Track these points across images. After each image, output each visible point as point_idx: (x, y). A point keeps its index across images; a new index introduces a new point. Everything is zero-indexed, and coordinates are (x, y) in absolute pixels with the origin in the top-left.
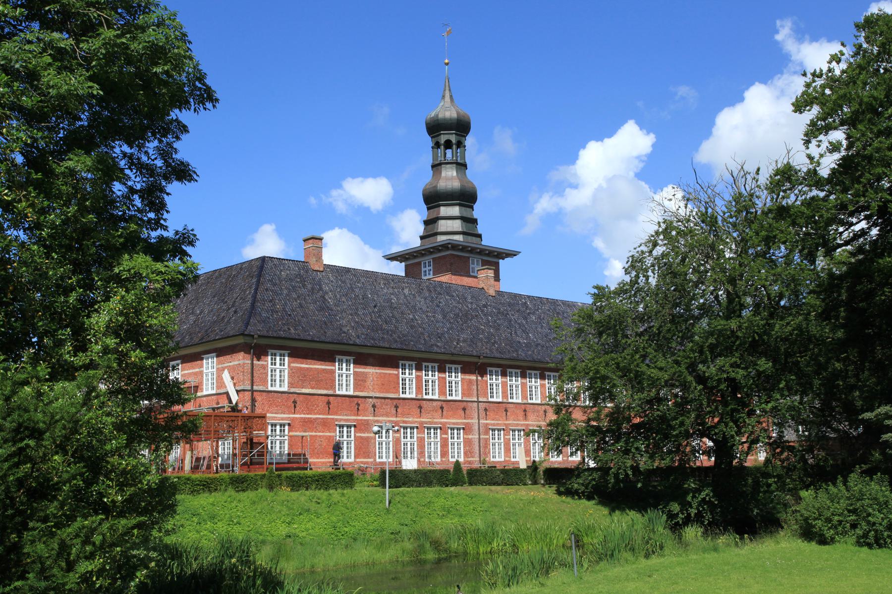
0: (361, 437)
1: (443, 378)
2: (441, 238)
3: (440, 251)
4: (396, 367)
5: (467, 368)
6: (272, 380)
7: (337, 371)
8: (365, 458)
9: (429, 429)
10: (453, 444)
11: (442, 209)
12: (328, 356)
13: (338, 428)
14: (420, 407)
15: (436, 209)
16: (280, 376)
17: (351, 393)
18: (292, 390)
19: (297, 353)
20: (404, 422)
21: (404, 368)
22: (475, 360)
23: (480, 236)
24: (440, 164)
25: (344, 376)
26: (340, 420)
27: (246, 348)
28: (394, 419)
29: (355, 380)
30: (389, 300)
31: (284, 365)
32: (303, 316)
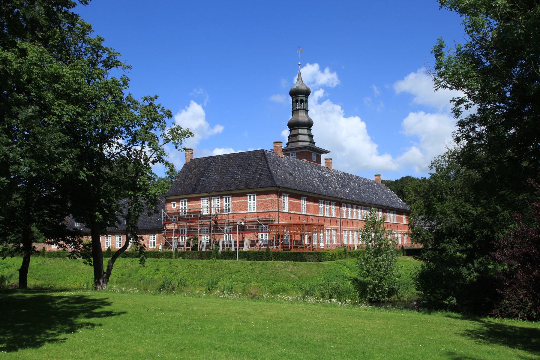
4: (318, 202)
11: (300, 130)
23: (314, 143)
24: (298, 110)
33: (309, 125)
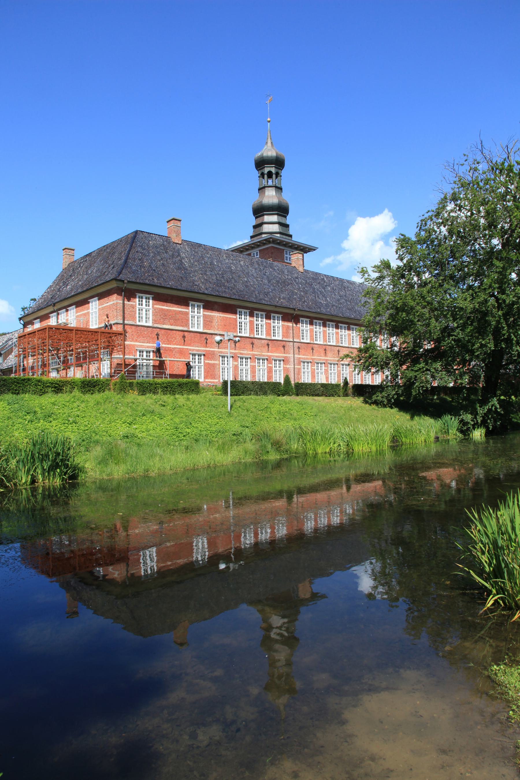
0: (209, 363)
1: (269, 323)
3: (264, 244)
4: (235, 313)
5: (286, 317)
6: (139, 317)
7: (190, 313)
8: (212, 379)
9: (259, 359)
10: (276, 371)
12: (184, 302)
13: (191, 356)
14: (253, 344)
15: (261, 218)
16: (146, 314)
17: (201, 330)
18: (156, 325)
19: (159, 298)
20: (241, 354)
21: (240, 314)
22: (292, 312)
23: (291, 236)
24: (264, 187)
25: (196, 317)
26: (193, 350)
27: (119, 291)
28: (233, 351)
29: (204, 320)
30: (230, 267)
31: (149, 306)
32: (164, 272)
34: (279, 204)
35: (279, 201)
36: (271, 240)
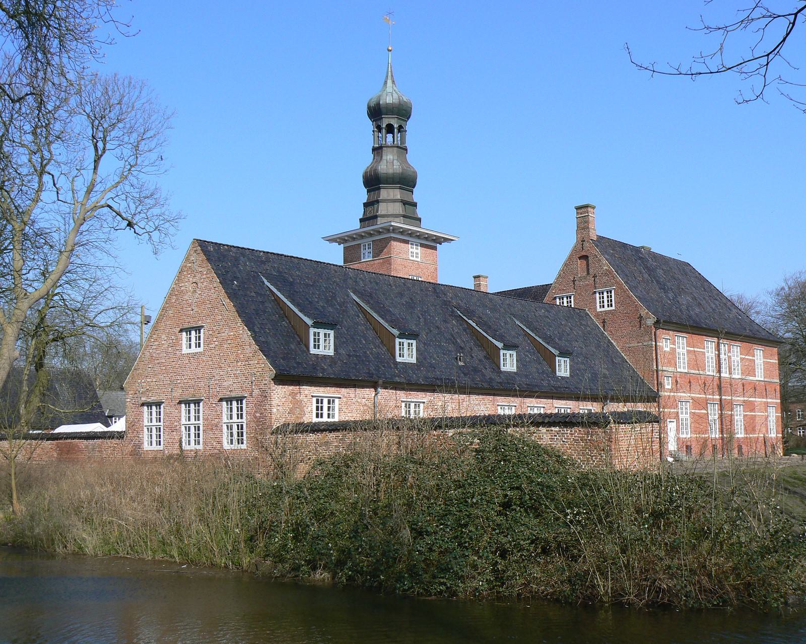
2: (381, 223)
23: (420, 220)
33: (407, 182)
34: (402, 173)
35: (403, 169)
36: (391, 228)
